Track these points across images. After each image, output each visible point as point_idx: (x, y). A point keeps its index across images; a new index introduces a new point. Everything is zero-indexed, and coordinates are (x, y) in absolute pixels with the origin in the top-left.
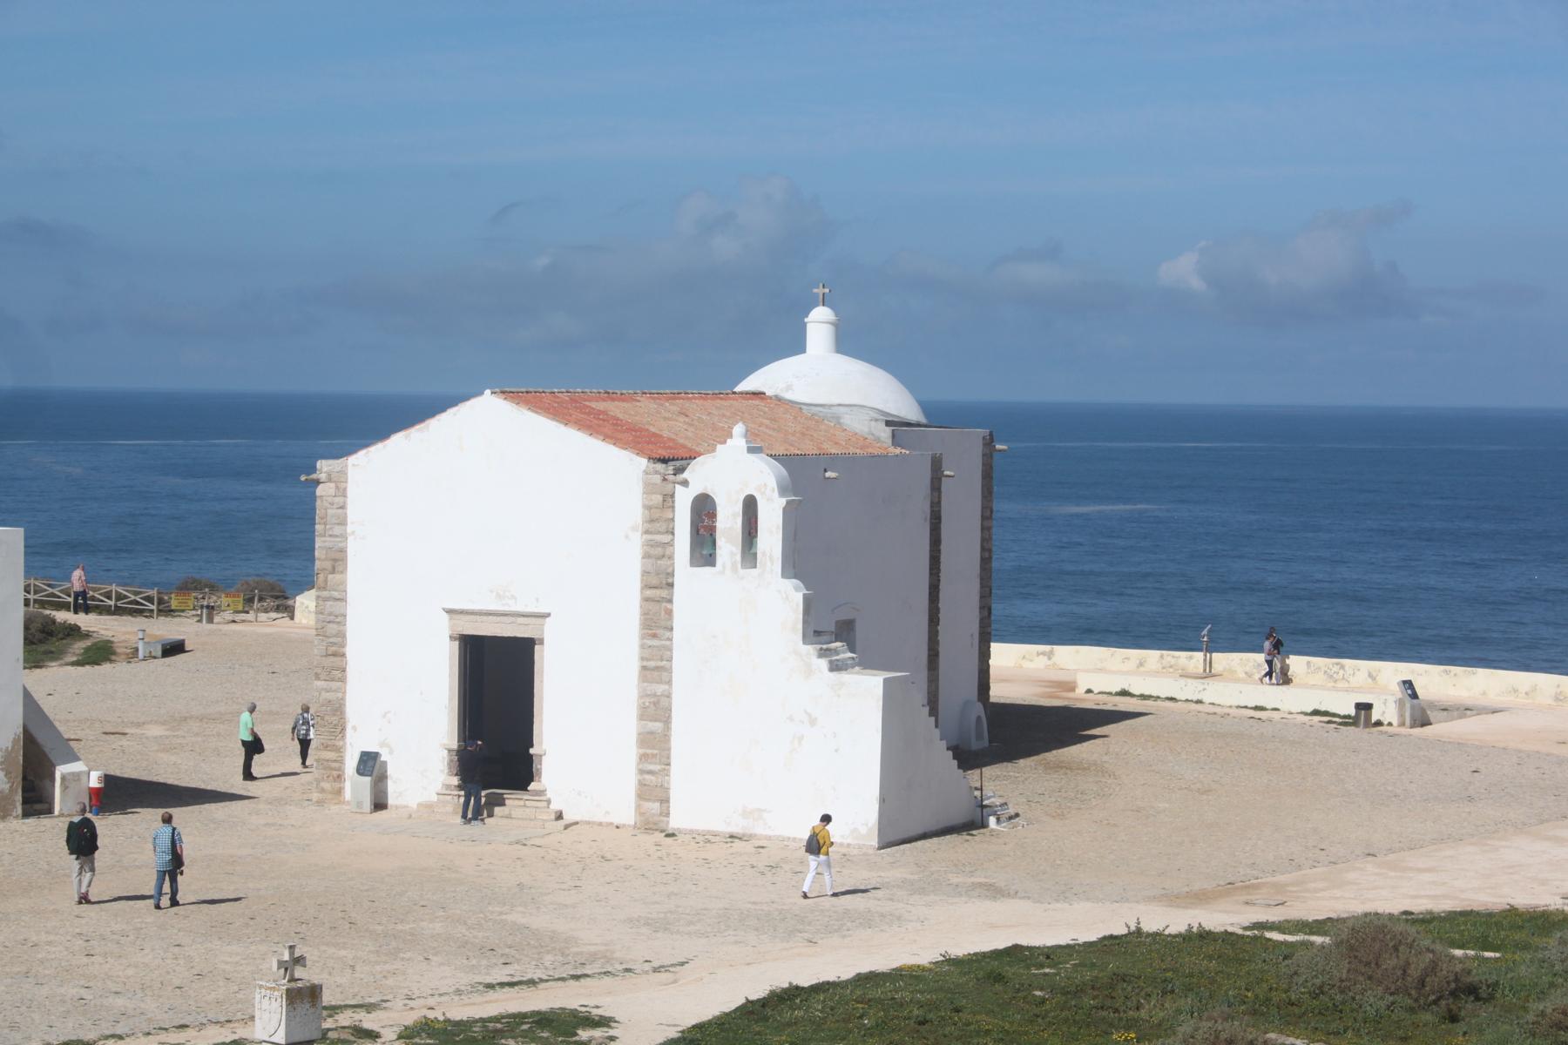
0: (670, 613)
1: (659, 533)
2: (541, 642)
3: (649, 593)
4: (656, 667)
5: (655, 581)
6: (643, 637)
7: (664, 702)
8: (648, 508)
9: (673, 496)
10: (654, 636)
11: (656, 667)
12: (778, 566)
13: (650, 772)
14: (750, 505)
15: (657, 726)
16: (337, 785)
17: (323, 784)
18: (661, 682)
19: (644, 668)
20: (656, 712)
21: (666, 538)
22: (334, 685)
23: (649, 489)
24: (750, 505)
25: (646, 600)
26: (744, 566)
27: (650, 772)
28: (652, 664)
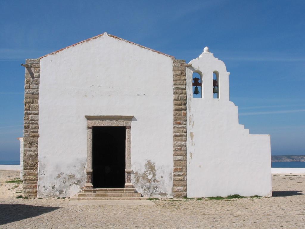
0: (185, 115)
1: (180, 85)
2: (130, 128)
3: (177, 107)
4: (180, 135)
5: (179, 102)
6: (174, 124)
7: (183, 148)
8: (175, 75)
9: (184, 71)
10: (180, 124)
11: (180, 135)
12: (228, 97)
13: (179, 175)
14: (216, 74)
15: (181, 157)
16: (35, 190)
17: (28, 190)
18: (182, 141)
19: (175, 136)
20: (181, 152)
21: (183, 87)
22: (33, 149)
23: (175, 69)
24: (216, 74)
25: (176, 110)
26: (214, 97)
27: (179, 175)
28: (178, 134)
